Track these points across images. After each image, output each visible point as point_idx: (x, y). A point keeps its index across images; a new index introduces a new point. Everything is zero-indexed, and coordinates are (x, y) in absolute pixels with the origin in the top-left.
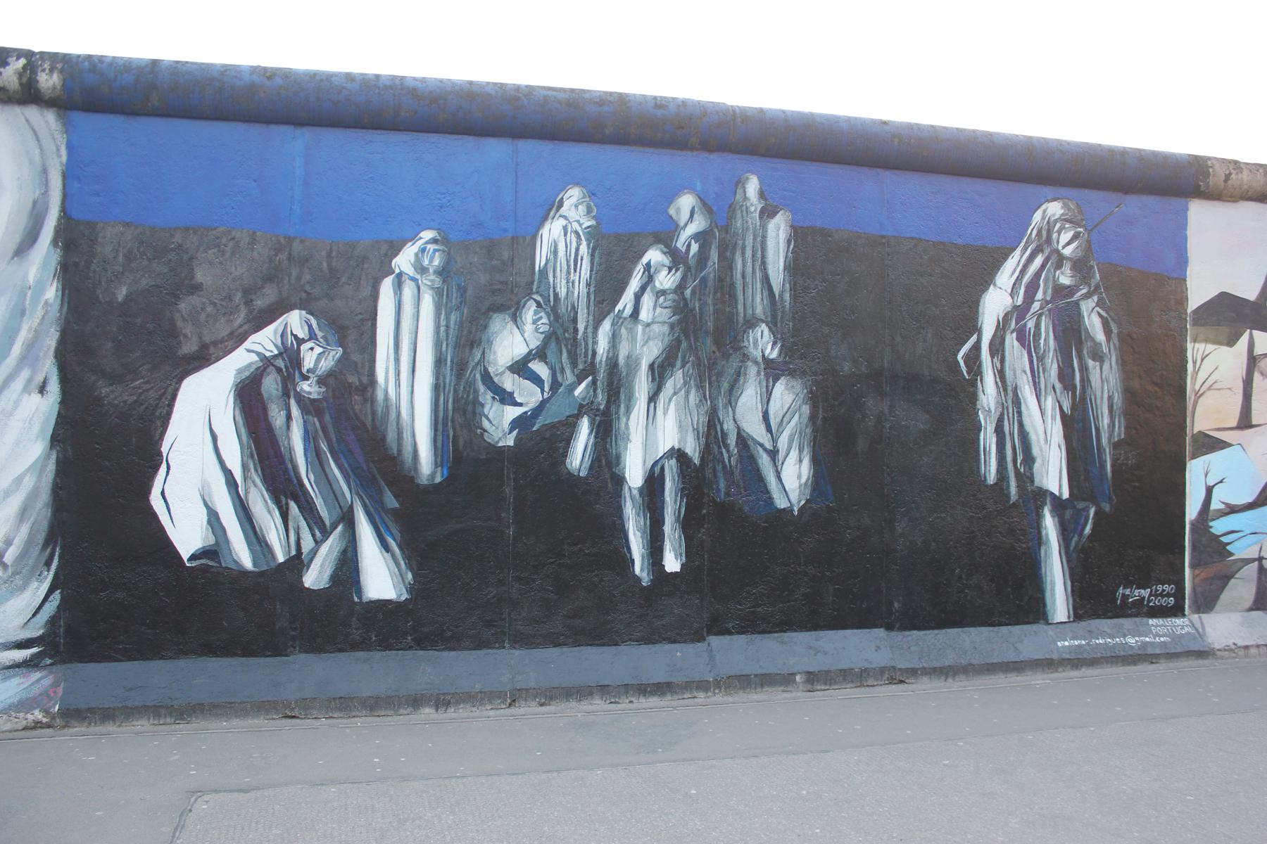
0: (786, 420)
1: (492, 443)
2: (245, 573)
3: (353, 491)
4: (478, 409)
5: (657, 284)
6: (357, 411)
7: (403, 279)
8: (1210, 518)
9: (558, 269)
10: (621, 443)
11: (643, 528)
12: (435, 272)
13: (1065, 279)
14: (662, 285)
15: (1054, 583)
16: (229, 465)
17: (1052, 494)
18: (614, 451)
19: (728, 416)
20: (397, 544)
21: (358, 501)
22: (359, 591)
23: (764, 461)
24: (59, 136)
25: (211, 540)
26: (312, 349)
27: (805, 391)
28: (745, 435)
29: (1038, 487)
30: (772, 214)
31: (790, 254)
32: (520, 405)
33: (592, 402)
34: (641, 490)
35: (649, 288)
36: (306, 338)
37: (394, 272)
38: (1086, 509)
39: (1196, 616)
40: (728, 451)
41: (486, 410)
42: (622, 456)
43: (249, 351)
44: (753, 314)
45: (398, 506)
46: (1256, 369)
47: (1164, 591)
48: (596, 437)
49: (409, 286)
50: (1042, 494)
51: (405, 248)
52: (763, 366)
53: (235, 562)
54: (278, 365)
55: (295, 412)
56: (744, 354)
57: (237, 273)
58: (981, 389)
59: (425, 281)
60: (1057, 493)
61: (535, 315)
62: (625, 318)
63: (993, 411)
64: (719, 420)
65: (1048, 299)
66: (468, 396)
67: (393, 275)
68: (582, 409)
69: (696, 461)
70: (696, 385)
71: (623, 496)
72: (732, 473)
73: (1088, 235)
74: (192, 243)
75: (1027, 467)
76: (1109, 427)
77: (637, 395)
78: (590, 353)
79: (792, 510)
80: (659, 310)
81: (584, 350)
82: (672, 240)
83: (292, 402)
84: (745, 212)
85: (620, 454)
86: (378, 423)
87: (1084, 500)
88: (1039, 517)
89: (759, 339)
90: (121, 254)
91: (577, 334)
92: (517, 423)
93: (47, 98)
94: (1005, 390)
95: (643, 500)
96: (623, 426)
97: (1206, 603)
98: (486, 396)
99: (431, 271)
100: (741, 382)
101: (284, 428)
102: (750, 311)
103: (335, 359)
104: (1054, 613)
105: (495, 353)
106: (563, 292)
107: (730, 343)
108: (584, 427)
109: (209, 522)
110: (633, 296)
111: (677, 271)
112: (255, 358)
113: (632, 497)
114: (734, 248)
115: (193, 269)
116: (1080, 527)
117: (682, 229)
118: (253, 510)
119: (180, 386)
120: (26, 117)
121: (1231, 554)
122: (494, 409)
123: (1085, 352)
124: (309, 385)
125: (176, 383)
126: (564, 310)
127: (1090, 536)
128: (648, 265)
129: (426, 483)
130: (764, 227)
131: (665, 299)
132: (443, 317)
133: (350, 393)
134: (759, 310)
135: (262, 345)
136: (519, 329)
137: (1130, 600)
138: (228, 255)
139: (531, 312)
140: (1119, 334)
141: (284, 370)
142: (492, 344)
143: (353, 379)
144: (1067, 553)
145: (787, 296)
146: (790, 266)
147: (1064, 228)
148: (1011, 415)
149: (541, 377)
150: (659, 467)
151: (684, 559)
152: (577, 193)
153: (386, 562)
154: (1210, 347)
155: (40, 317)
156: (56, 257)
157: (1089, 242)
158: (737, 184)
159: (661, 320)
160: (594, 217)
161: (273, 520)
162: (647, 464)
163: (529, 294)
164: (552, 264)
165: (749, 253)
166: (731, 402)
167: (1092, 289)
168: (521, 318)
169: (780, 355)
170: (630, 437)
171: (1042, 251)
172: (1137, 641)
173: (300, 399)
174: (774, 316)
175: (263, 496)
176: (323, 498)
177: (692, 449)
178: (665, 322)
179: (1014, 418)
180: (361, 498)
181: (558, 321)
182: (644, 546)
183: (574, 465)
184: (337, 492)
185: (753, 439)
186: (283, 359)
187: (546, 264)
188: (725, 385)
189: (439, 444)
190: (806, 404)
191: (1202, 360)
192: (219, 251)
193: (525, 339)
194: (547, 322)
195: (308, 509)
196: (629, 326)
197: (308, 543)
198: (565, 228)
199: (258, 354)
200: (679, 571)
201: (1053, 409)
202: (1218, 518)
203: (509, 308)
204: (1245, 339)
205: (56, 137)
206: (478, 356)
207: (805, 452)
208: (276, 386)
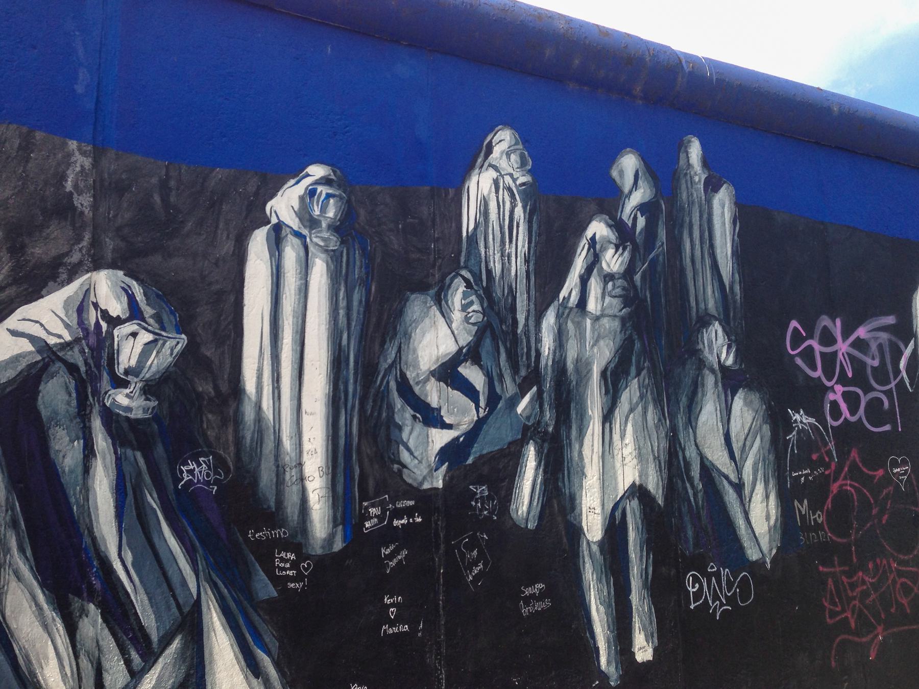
0: (748, 443)
1: (415, 484)
3: (201, 574)
4: (394, 433)
5: (604, 265)
6: (212, 439)
7: (283, 233)
9: (491, 237)
10: (576, 481)
12: (329, 227)
14: (609, 265)
18: (567, 491)
21: (210, 592)
23: (730, 496)
26: (134, 335)
27: (764, 407)
28: (708, 464)
30: (716, 190)
32: (449, 427)
33: (539, 422)
34: (601, 544)
35: (595, 271)
36: (123, 317)
41: (405, 436)
42: (577, 496)
43: (14, 333)
45: (275, 594)
48: (545, 472)
49: (293, 246)
51: (286, 186)
52: (719, 375)
54: (72, 361)
55: (101, 441)
62: (571, 309)
64: (680, 444)
66: (380, 414)
67: (268, 226)
69: (660, 501)
71: (581, 554)
72: (699, 518)
77: (590, 413)
78: (533, 354)
79: (765, 562)
80: (608, 299)
81: (525, 350)
83: (97, 424)
85: (575, 494)
86: (245, 458)
89: (714, 340)
91: (517, 327)
96: (576, 454)
98: (404, 414)
99: (324, 225)
100: (700, 395)
101: (80, 470)
102: (702, 306)
105: (415, 350)
106: (497, 269)
110: (578, 280)
111: (624, 250)
112: (26, 346)
113: (591, 556)
114: (682, 226)
117: (626, 197)
122: (415, 434)
124: (127, 396)
126: (499, 293)
128: (593, 238)
129: (319, 551)
130: (709, 202)
131: (614, 285)
132: (342, 294)
135: (42, 325)
141: (83, 369)
142: (410, 337)
143: (205, 387)
145: (737, 288)
146: (737, 251)
149: (474, 387)
150: (619, 511)
151: (656, 640)
152: (508, 138)
159: (610, 312)
160: (529, 171)
161: (52, 641)
162: (606, 507)
163: (455, 267)
165: (696, 234)
166: (691, 421)
168: (447, 302)
169: (735, 362)
170: (585, 470)
173: (110, 418)
176: (147, 593)
177: (654, 484)
178: (615, 316)
180: (214, 586)
181: (493, 309)
182: (609, 626)
183: (520, 512)
184: (175, 580)
185: (718, 470)
186: (82, 352)
187: (476, 228)
188: (684, 401)
189: (340, 489)
190: (766, 423)
193: (453, 333)
194: (480, 309)
196: (576, 320)
198: (496, 182)
199: (32, 339)
200: (651, 659)
207: (771, 486)
208: (67, 398)
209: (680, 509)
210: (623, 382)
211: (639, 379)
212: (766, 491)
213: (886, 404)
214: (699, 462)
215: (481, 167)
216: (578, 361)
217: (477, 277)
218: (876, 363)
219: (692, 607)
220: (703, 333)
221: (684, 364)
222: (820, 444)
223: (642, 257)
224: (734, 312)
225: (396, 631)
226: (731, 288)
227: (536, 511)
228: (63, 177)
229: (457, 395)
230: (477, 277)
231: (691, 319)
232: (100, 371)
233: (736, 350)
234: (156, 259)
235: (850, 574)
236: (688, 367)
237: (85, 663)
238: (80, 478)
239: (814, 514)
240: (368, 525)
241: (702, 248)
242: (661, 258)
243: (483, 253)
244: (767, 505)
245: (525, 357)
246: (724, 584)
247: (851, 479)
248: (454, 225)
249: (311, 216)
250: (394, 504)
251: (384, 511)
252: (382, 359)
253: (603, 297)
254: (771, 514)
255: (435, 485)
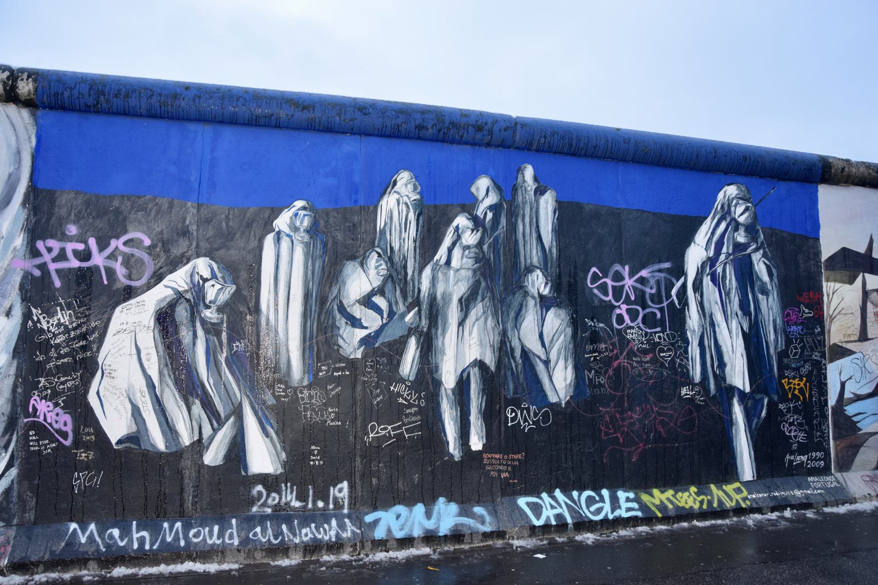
0: (555, 338)
2: (160, 454)
3: (242, 392)
7: (281, 235)
8: (844, 404)
10: (439, 356)
11: (455, 418)
13: (741, 238)
14: (467, 241)
15: (743, 453)
16: (149, 372)
17: (739, 389)
18: (434, 362)
19: (515, 335)
20: (274, 431)
22: (246, 468)
23: (540, 368)
24: (31, 128)
25: (134, 428)
26: (213, 286)
27: (568, 318)
28: (527, 350)
29: (729, 385)
30: (543, 193)
31: (555, 220)
32: (366, 328)
33: (418, 326)
34: (453, 390)
35: (458, 244)
36: (209, 278)
37: (274, 231)
38: (762, 399)
39: (839, 474)
40: (515, 361)
41: (341, 332)
43: (166, 286)
44: (531, 263)
46: (868, 300)
47: (816, 456)
48: (421, 352)
50: (731, 390)
51: (283, 213)
52: (538, 300)
53: (153, 446)
55: (200, 332)
56: (525, 291)
57: (158, 230)
58: (688, 315)
59: (297, 237)
60: (742, 388)
61: (377, 262)
62: (441, 266)
63: (697, 331)
64: (508, 338)
65: (730, 252)
66: (328, 321)
68: (411, 331)
69: (493, 368)
70: (492, 314)
73: (755, 209)
74: (127, 207)
75: (721, 370)
76: (774, 341)
77: (450, 321)
78: (416, 290)
79: (561, 404)
80: (465, 260)
81: (412, 288)
82: (473, 210)
83: (198, 324)
84: (524, 191)
87: (761, 393)
88: (730, 405)
90: (73, 214)
91: (407, 276)
92: (364, 341)
93: (23, 99)
94: (704, 316)
95: (455, 398)
96: (440, 343)
97: (845, 465)
98: (341, 322)
99: (302, 230)
100: (524, 311)
101: (191, 344)
102: (529, 261)
103: (231, 293)
104: (743, 474)
105: (348, 290)
106: (396, 247)
107: (516, 283)
108: (412, 343)
109: (133, 415)
111: (477, 232)
112: (170, 292)
114: (517, 216)
115: (126, 226)
116: (758, 413)
117: (481, 202)
118: (166, 405)
119: (113, 313)
120: (6, 114)
121: (860, 429)
122: (347, 331)
123: (756, 289)
124: (211, 313)
125: (111, 310)
126: (397, 259)
127: (765, 418)
128: (457, 228)
129: (296, 385)
130: (537, 201)
131: (469, 252)
132: (310, 263)
133: (241, 318)
134: (535, 260)
136: (365, 272)
137: (794, 464)
138: (153, 213)
139: (374, 261)
140: (778, 275)
141: (192, 301)
142: (345, 283)
144: (750, 431)
145: (554, 250)
146: (556, 228)
147: (739, 203)
148: (709, 333)
152: (407, 176)
153: (266, 445)
154: (838, 285)
155: (10, 259)
156: (23, 215)
157: (755, 213)
158: (518, 172)
159: (467, 267)
161: (182, 413)
163: (372, 245)
164: (389, 226)
165: (527, 220)
166: (517, 326)
167: (759, 245)
168: (367, 265)
169: (550, 292)
171: (725, 219)
172: (802, 493)
173: (203, 322)
174: (546, 264)
175: (174, 395)
176: (219, 397)
177: (490, 360)
178: (469, 269)
179: (711, 336)
182: (456, 431)
186: (192, 294)
188: (512, 314)
190: (569, 327)
191: (833, 294)
192: (146, 212)
193: (369, 281)
194: (386, 268)
195: (208, 405)
197: (207, 431)
198: (398, 201)
199: (173, 289)
201: (737, 329)
202: (850, 404)
203: (358, 257)
204: (859, 279)
205: (28, 128)
206: (335, 291)
209: (505, 375)
210: (472, 305)
211: (483, 304)
212: (566, 366)
213: (659, 315)
214: (520, 348)
215: (390, 193)
216: (444, 293)
217: (385, 251)
218: (654, 291)
219: (509, 425)
220: (528, 276)
221: (514, 294)
222: (607, 338)
223: (489, 235)
224: (551, 264)
225: (334, 424)
226: (550, 250)
227: (415, 370)
228: (185, 219)
229: (371, 312)
230: (385, 251)
231: (520, 270)
232: (199, 302)
233: (551, 286)
234: (222, 252)
235: (621, 413)
236: (517, 296)
237: (195, 424)
238: (192, 347)
239: (599, 378)
240: (321, 374)
241: (530, 228)
242: (502, 235)
243: (389, 239)
244: (566, 372)
245: (411, 293)
246: (532, 414)
247: (628, 359)
248: (372, 225)
249: (295, 225)
250: (334, 365)
251: (329, 368)
252: (330, 294)
253: (462, 258)
254: (568, 377)
255: (357, 357)
